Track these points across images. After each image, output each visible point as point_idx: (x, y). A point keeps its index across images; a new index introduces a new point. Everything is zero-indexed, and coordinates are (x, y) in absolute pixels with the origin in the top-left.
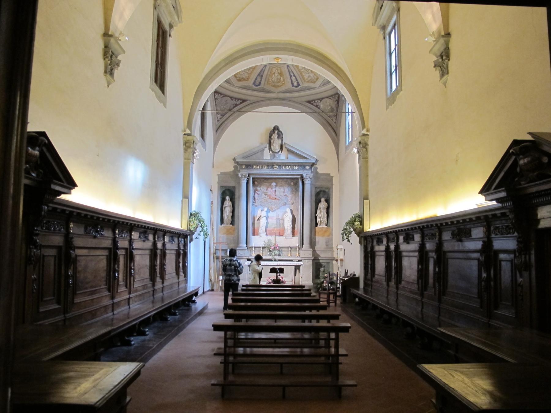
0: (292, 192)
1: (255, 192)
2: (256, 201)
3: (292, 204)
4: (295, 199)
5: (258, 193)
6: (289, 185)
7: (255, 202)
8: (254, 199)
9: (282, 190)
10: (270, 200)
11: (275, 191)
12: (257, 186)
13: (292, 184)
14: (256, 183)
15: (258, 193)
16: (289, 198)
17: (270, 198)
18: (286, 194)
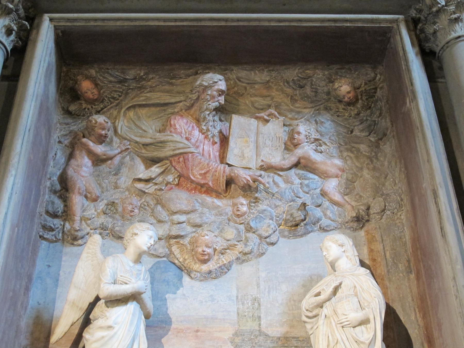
0: (348, 144)
1: (73, 148)
2: (77, 201)
3: (360, 221)
4: (377, 191)
5: (99, 149)
6: (324, 103)
7: (66, 214)
8: (64, 187)
9: (275, 129)
10: (181, 199)
11: (224, 140)
12: (100, 104)
13: (344, 88)
14: (86, 86)
15: (99, 149)
16: (332, 186)
17: (183, 181)
18: (307, 150)
